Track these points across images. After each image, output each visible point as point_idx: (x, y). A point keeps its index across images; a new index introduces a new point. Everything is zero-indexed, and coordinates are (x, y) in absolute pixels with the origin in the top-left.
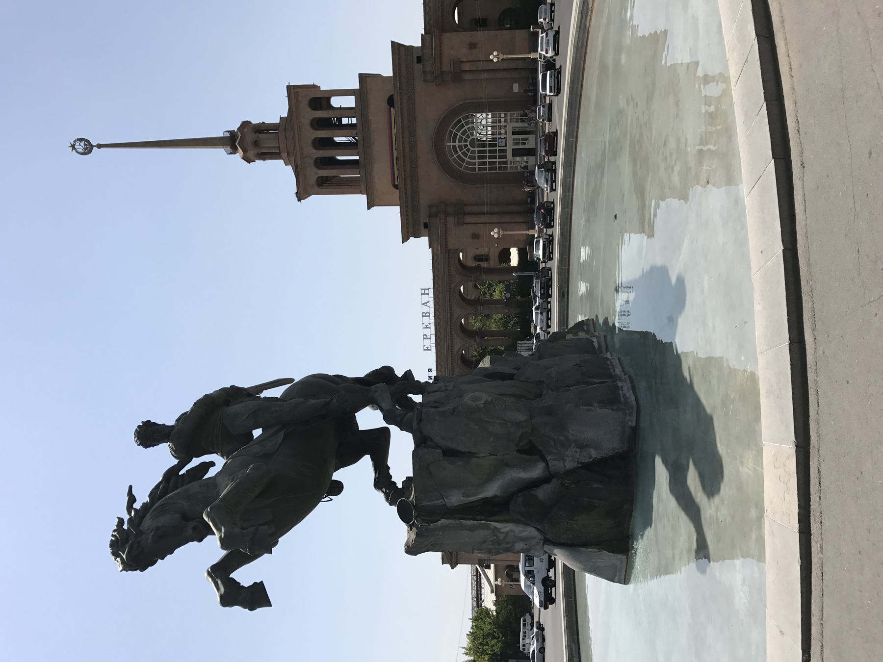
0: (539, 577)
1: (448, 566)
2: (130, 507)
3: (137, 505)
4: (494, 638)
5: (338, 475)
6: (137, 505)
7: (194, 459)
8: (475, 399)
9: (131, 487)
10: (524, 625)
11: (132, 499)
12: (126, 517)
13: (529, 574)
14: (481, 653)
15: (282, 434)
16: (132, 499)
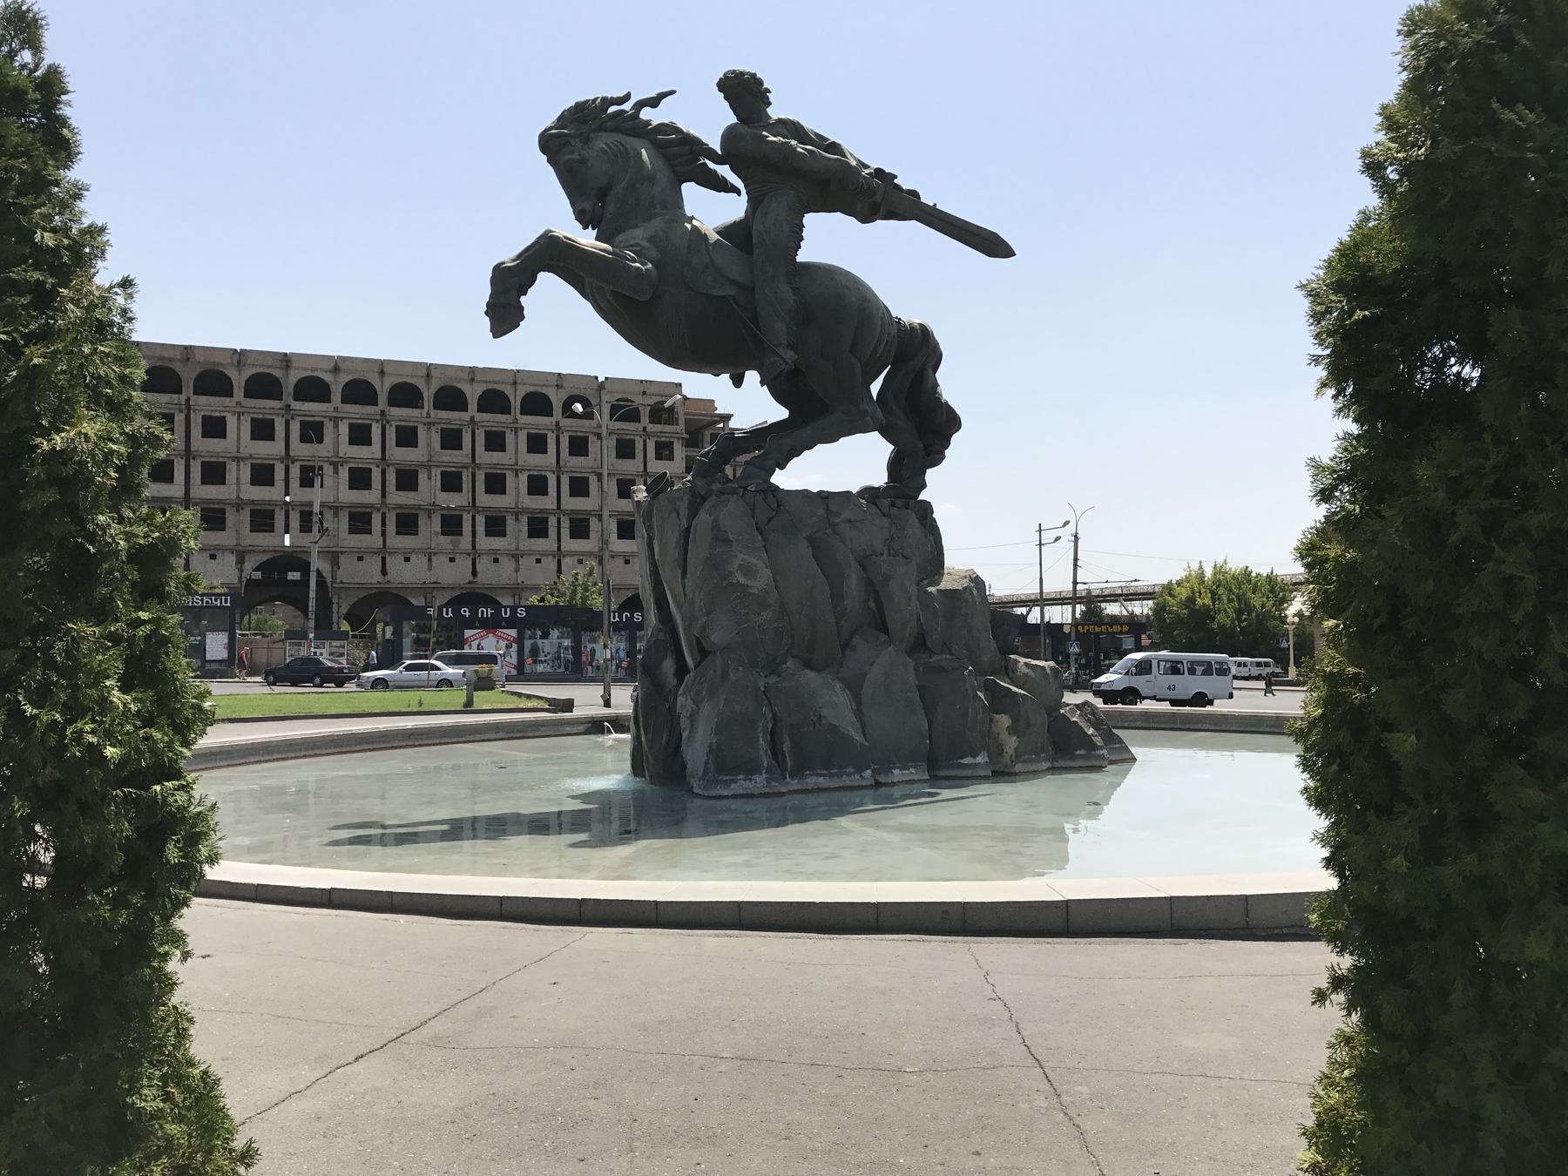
0: (1139, 682)
2: (641, 105)
3: (646, 114)
4: (1239, 612)
5: (752, 377)
6: (646, 114)
7: (727, 167)
8: (749, 571)
9: (672, 92)
10: (1259, 664)
11: (654, 102)
13: (1143, 668)
14: (1214, 593)
15: (729, 291)
16: (654, 102)
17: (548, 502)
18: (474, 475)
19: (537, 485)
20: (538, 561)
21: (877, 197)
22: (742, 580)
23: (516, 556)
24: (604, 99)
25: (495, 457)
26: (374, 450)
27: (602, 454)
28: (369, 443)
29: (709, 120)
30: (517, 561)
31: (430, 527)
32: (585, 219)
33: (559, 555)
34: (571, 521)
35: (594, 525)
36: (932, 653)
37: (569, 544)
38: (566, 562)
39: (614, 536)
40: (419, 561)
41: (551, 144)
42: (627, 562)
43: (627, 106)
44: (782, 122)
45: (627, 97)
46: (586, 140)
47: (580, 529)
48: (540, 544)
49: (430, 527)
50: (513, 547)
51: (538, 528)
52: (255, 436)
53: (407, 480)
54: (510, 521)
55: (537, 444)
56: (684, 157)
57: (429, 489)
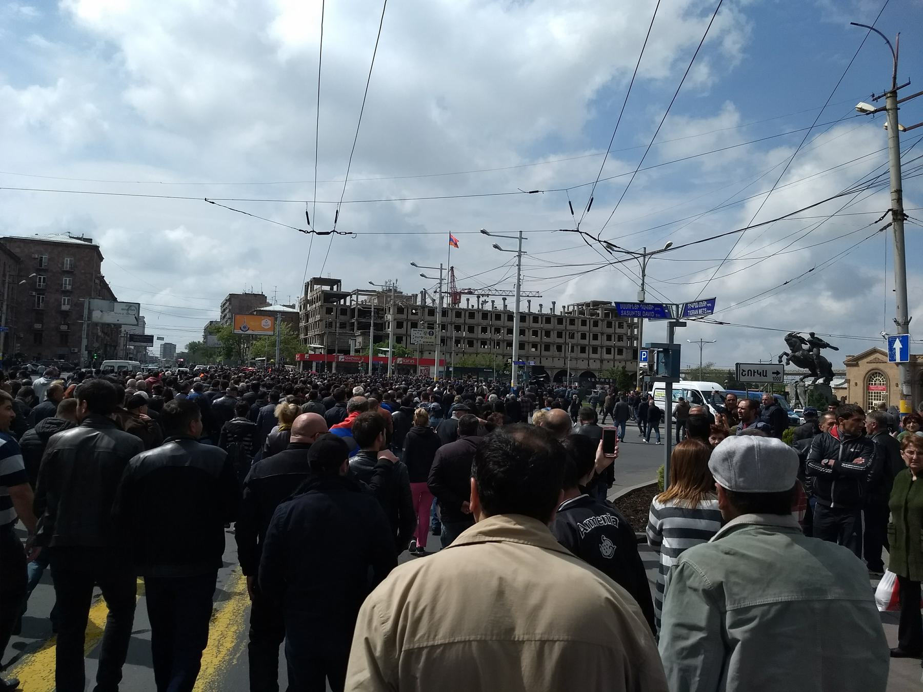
1: (845, 359)
17: (586, 342)
19: (583, 336)
25: (572, 327)
31: (553, 349)
33: (589, 359)
35: (599, 349)
37: (592, 356)
38: (591, 361)
40: (550, 359)
47: (595, 350)
48: (583, 355)
49: (553, 349)
52: (509, 320)
53: (548, 334)
56: (802, 341)
57: (554, 337)
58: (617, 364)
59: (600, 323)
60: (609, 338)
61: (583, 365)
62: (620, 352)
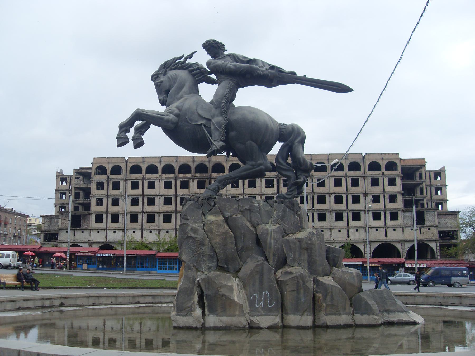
2: (186, 59)
3: (189, 61)
6: (189, 61)
7: (213, 75)
8: (195, 231)
9: (196, 52)
11: (191, 56)
12: (182, 60)
15: (203, 122)
16: (191, 56)
17: (342, 207)
18: (313, 197)
19: (338, 200)
20: (340, 231)
21: (274, 77)
22: (193, 235)
23: (330, 229)
24: (174, 59)
25: (321, 189)
26: (274, 190)
27: (365, 185)
28: (273, 187)
29: (202, 59)
30: (331, 231)
32: (163, 103)
33: (348, 228)
34: (353, 213)
36: (290, 266)
38: (351, 231)
39: (371, 218)
41: (155, 77)
42: (377, 230)
43: (182, 60)
44: (229, 55)
45: (183, 55)
46: (165, 74)
47: (356, 217)
48: (340, 224)
50: (329, 225)
51: (339, 217)
54: (328, 214)
55: (338, 183)
58: (390, 231)
59: (361, 182)
60: (376, 199)
61: (380, 236)
62: (394, 216)
